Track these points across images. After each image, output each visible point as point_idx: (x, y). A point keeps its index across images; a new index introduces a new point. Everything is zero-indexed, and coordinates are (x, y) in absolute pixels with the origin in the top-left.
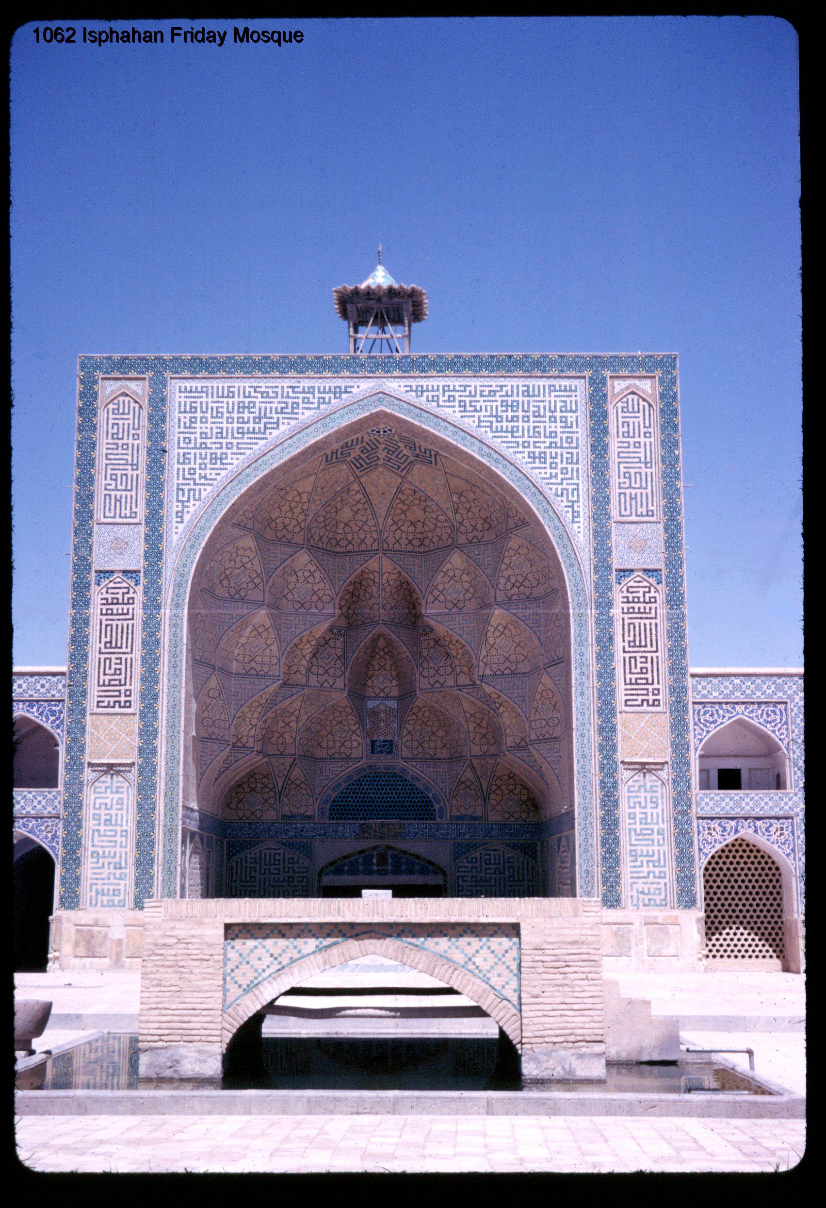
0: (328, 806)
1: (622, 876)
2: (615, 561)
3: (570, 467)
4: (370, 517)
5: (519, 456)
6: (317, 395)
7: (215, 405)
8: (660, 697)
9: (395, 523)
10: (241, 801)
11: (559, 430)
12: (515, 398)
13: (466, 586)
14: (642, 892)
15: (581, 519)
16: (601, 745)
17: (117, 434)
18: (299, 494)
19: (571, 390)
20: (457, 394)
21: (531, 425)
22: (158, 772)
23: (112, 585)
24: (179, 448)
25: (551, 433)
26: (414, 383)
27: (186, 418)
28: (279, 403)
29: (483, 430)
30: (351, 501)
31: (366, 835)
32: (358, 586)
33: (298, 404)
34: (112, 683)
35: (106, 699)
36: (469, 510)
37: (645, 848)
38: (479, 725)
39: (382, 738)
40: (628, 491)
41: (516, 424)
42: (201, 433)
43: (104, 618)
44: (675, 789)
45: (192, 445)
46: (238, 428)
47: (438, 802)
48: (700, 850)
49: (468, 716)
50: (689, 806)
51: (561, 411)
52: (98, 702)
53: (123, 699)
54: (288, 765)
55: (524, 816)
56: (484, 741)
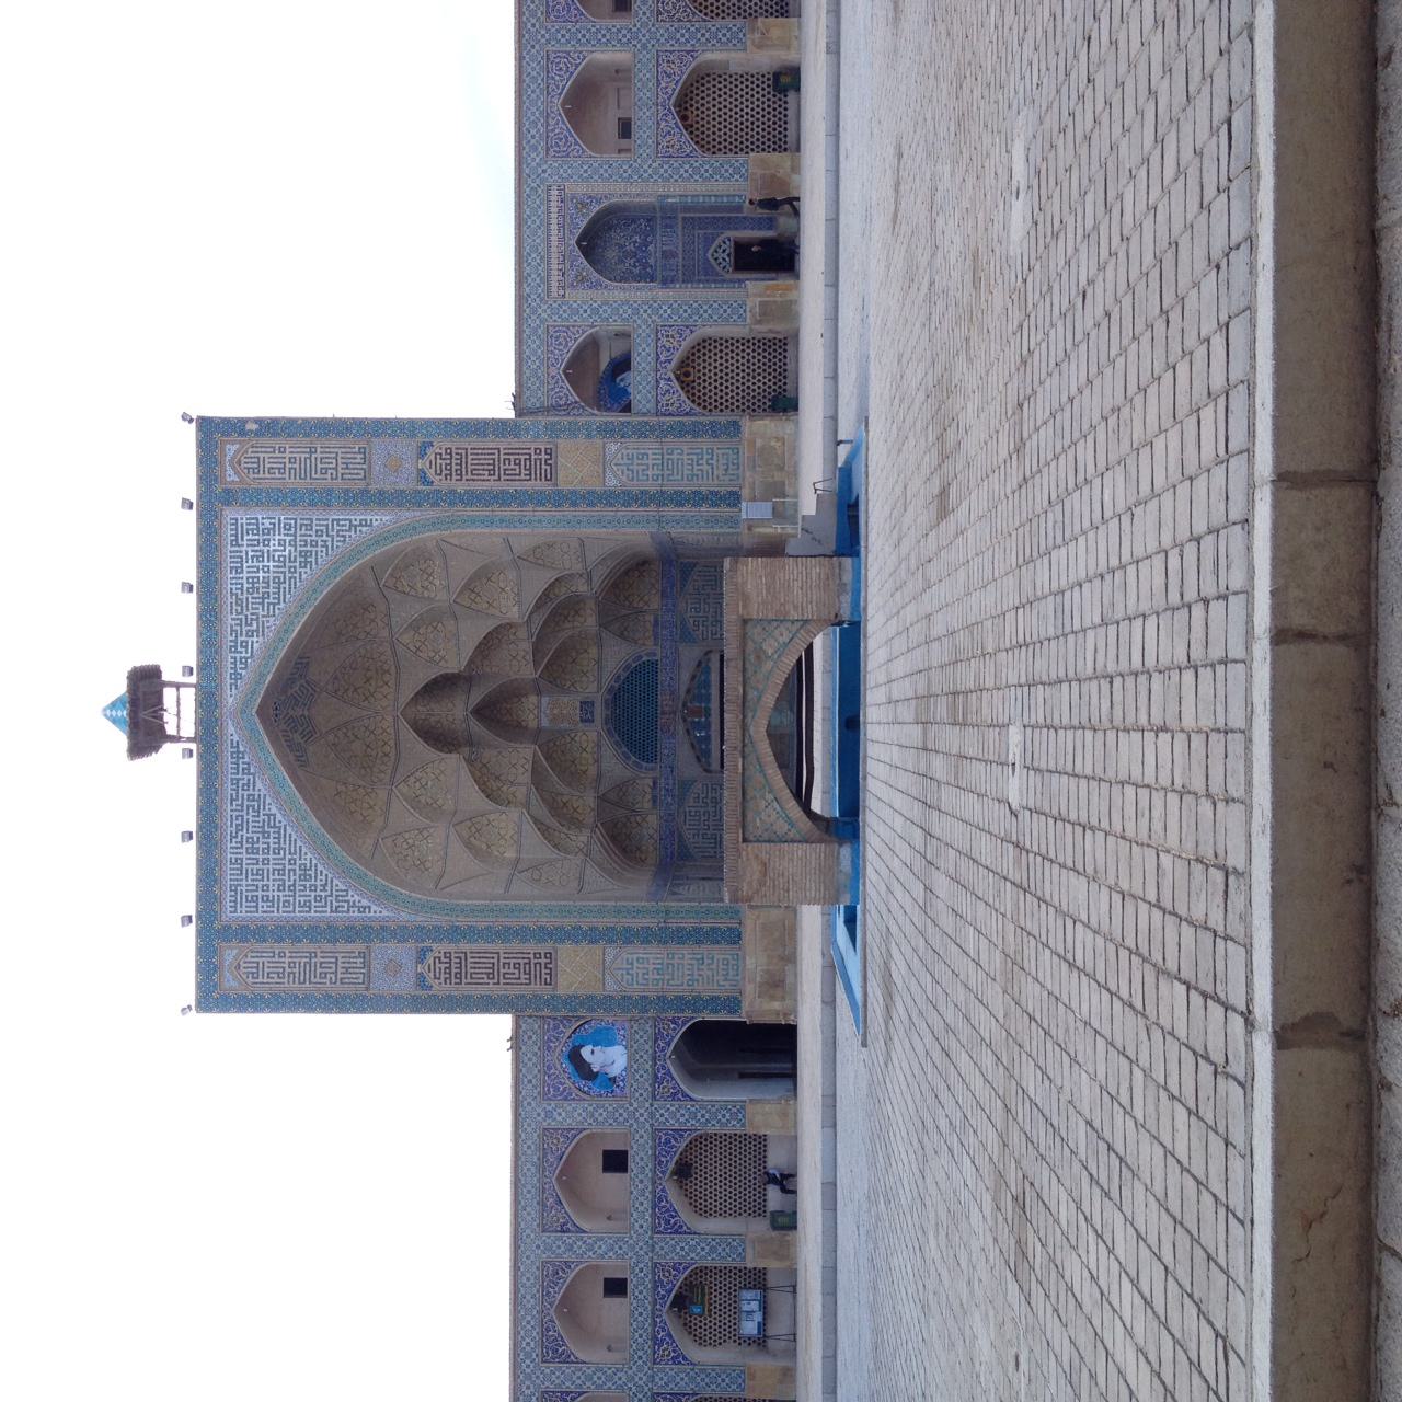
0: (644, 764)
5: (304, 576)
6: (240, 776)
7: (250, 877)
10: (638, 849)
11: (277, 537)
14: (726, 470)
15: (369, 518)
17: (278, 973)
20: (239, 639)
21: (271, 564)
22: (612, 925)
23: (431, 974)
24: (294, 912)
25: (279, 544)
28: (248, 813)
31: (672, 728)
34: (527, 971)
35: (544, 976)
37: (686, 467)
38: (566, 618)
39: (578, 712)
40: (340, 471)
41: (271, 578)
42: (279, 890)
43: (464, 981)
44: (630, 436)
45: (291, 899)
46: (274, 853)
47: (641, 657)
48: (687, 414)
49: (557, 629)
50: (647, 423)
52: (546, 984)
53: (543, 961)
56: (581, 612)
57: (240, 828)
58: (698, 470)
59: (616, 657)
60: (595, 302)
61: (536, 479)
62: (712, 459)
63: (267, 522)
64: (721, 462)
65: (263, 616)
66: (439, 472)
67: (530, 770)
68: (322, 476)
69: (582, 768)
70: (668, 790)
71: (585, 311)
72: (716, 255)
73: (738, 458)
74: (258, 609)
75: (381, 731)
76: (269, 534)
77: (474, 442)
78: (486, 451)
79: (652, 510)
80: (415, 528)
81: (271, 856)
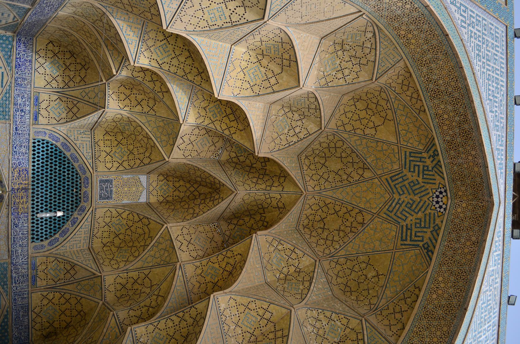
0: (47, 138)
4: (334, 185)
9: (326, 205)
10: (55, 55)
13: (285, 270)
18: (375, 127)
30: (350, 170)
31: (16, 174)
32: (261, 172)
36: (352, 270)
39: (114, 189)
47: (50, 244)
49: (146, 272)
54: (96, 101)
55: (38, 327)
56: (119, 287)
59: (75, 241)
67: (179, 137)
69: (109, 138)
70: (22, 111)
75: (314, 178)
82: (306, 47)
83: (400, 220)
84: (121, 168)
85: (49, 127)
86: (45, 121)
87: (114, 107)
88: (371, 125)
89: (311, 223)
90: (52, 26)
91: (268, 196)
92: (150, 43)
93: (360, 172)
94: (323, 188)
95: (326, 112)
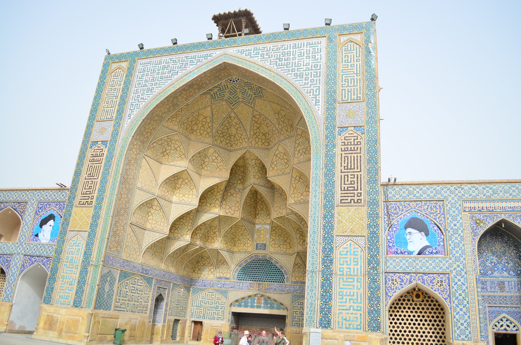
0: (236, 274)
1: (333, 308)
2: (338, 124)
3: (315, 78)
4: (243, 131)
5: (290, 76)
6: (197, 58)
8: (362, 198)
9: (255, 134)
10: (199, 270)
11: (311, 62)
12: (289, 50)
13: (286, 161)
14: (346, 319)
15: (320, 104)
16: (324, 226)
18: (205, 118)
19: (318, 43)
20: (260, 51)
21: (297, 61)
26: (240, 48)
27: (140, 75)
29: (272, 66)
30: (234, 123)
31: (252, 288)
33: (187, 63)
37: (348, 291)
39: (261, 242)
40: (346, 89)
47: (286, 274)
48: (386, 294)
49: (296, 230)
50: (378, 265)
51: (312, 53)
54: (216, 252)
57: (174, 61)
58: (346, 299)
60: (462, 232)
61: (342, 193)
62: (354, 310)
63: (319, 57)
64: (351, 316)
65: (270, 60)
66: (346, 138)
68: (344, 80)
71: (455, 225)
72: (504, 320)
73: (353, 328)
74: (274, 57)
76: (312, 58)
77: (364, 157)
78: (359, 164)
79: (320, 267)
80: (314, 127)
81: (160, 76)
82: (167, 171)
83: (252, 98)
84: (250, 239)
85: (232, 273)
86: (229, 274)
87: (218, 244)
88: (204, 120)
89: (267, 141)
90: (182, 272)
91: (255, 166)
92: (179, 235)
93: (233, 118)
94: (245, 137)
95: (200, 147)
